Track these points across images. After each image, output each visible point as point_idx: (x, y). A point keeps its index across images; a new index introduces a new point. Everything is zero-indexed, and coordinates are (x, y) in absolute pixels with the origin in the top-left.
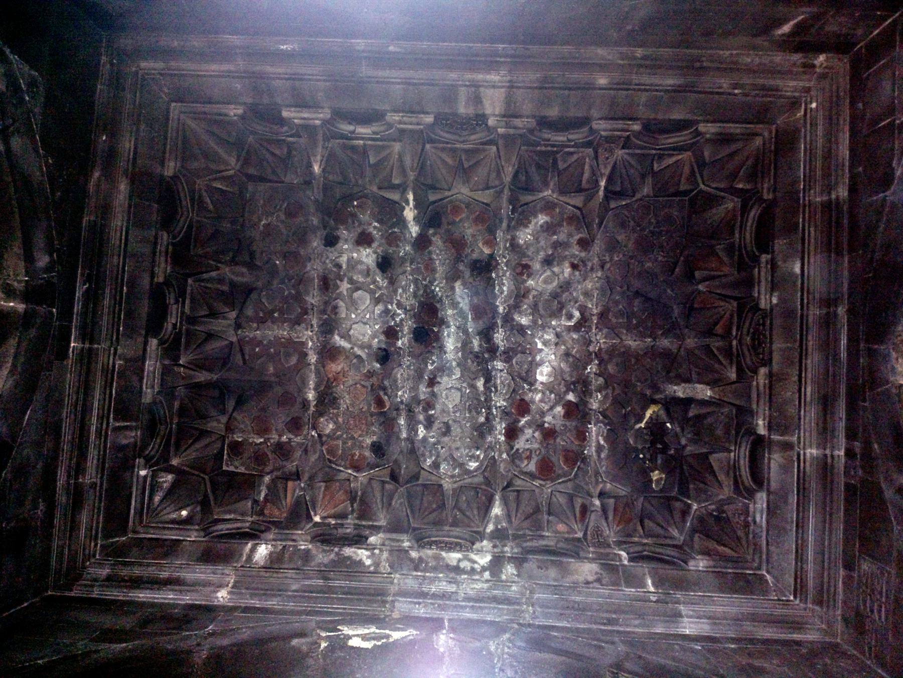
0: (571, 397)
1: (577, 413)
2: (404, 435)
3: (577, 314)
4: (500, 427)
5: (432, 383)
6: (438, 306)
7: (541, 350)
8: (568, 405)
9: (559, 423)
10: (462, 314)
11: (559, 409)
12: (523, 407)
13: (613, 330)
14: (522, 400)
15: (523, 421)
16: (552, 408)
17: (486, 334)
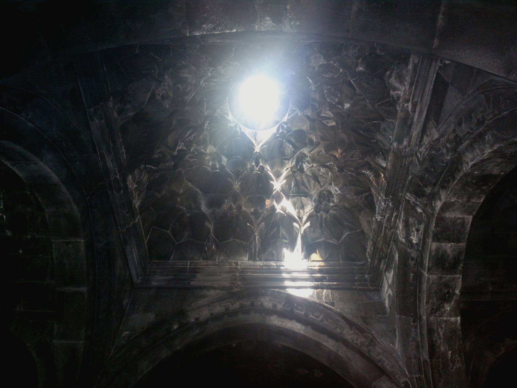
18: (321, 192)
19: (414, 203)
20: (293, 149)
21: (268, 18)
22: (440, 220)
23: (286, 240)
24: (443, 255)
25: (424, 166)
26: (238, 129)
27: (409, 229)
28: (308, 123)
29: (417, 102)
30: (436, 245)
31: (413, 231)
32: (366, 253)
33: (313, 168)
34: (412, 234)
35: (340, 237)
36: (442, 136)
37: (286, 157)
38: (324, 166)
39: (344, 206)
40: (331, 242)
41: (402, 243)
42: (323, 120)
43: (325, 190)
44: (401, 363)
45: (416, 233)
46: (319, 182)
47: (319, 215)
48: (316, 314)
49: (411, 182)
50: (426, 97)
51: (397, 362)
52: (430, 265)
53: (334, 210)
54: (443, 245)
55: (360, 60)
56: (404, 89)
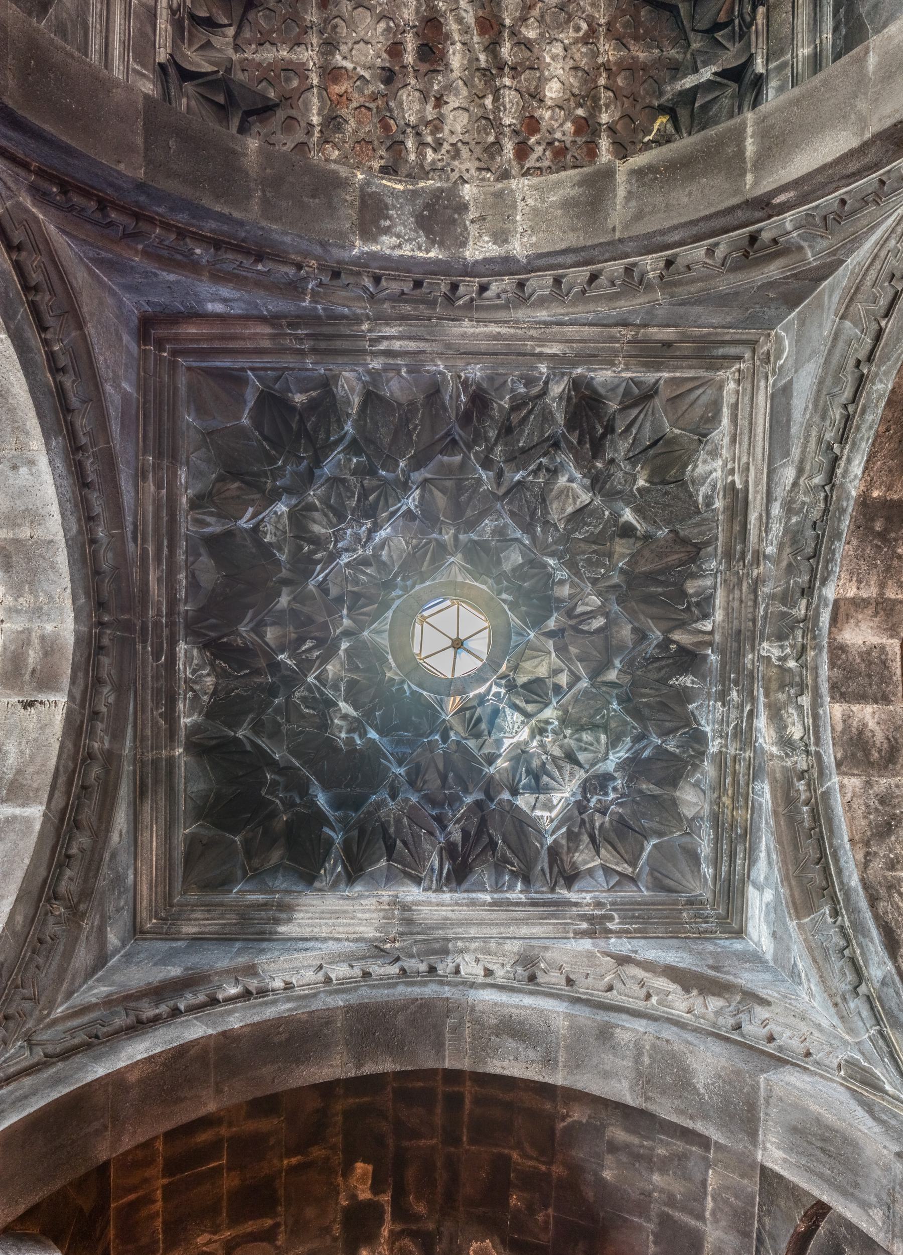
0: (580, 112)
1: (587, 128)
2: (412, 157)
3: (584, 26)
4: (509, 147)
5: (440, 102)
6: (442, 20)
7: (549, 64)
8: (577, 121)
9: (568, 139)
10: (466, 31)
11: (569, 126)
12: (532, 124)
13: (620, 42)
14: (532, 117)
15: (533, 140)
16: (561, 125)
17: (492, 48)
19: (780, 659)
22: (838, 651)
23: (513, 865)
24: (860, 733)
25: (784, 564)
26: (406, 687)
29: (748, 464)
30: (840, 709)
32: (698, 864)
33: (566, 741)
34: (790, 720)
39: (640, 792)
40: (619, 869)
41: (772, 755)
42: (581, 622)
46: (580, 765)
47: (585, 816)
50: (760, 444)
52: (839, 756)
54: (856, 708)
55: (638, 468)
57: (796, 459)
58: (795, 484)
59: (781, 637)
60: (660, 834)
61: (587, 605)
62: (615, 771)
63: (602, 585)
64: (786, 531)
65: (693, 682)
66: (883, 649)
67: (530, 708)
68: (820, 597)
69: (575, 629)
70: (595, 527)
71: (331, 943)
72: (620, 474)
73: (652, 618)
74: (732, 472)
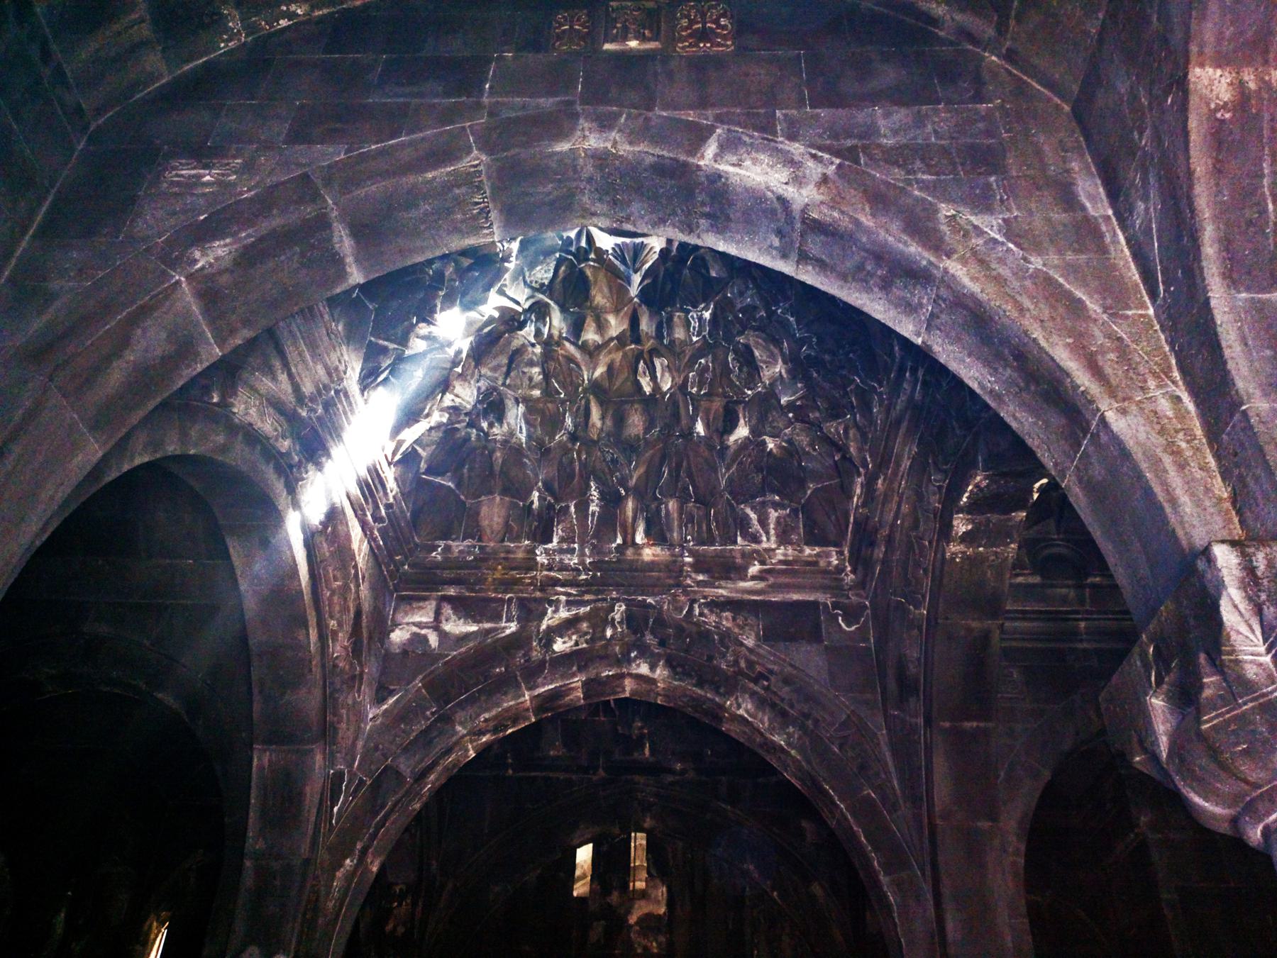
18: (495, 389)
19: (613, 619)
20: (546, 282)
21: (970, 527)
25: (684, 624)
27: (568, 629)
28: (625, 326)
31: (570, 638)
33: (530, 349)
35: (437, 474)
36: (751, 650)
37: (527, 274)
38: (546, 375)
39: (492, 452)
42: (645, 363)
43: (499, 394)
44: (360, 744)
45: (572, 643)
46: (507, 374)
48: (338, 574)
49: (644, 605)
51: (356, 739)
53: (478, 435)
56: (774, 546)
57: (761, 651)
58: (742, 644)
59: (629, 618)
60: (458, 485)
61: (662, 375)
62: (508, 424)
63: (680, 398)
64: (708, 631)
65: (593, 513)
66: (624, 691)
67: (558, 286)
68: (659, 656)
69: (638, 356)
70: (738, 377)
71: (283, 377)
72: (781, 425)
73: (646, 472)
74: (762, 563)
